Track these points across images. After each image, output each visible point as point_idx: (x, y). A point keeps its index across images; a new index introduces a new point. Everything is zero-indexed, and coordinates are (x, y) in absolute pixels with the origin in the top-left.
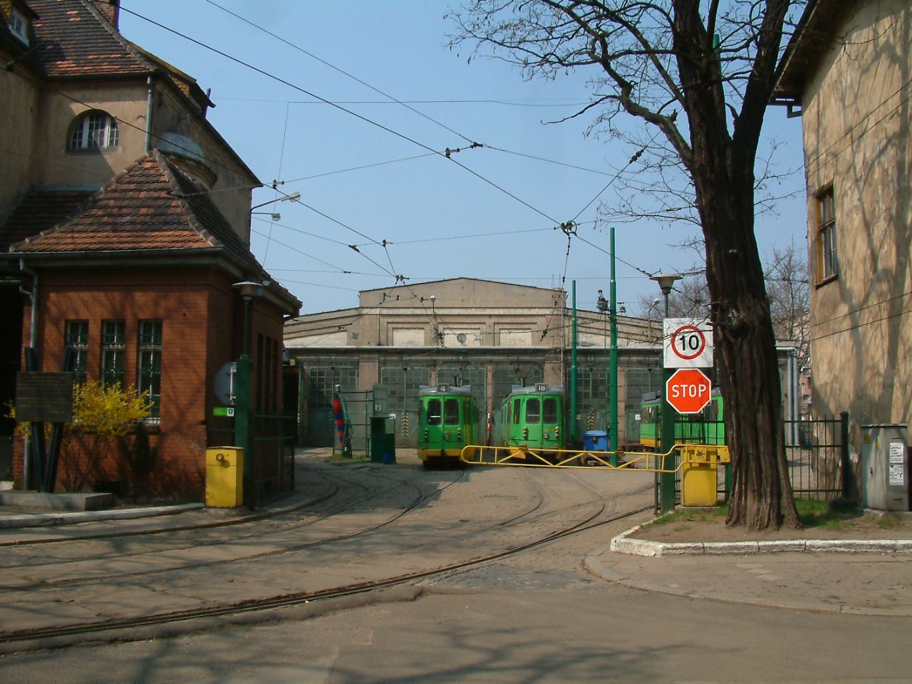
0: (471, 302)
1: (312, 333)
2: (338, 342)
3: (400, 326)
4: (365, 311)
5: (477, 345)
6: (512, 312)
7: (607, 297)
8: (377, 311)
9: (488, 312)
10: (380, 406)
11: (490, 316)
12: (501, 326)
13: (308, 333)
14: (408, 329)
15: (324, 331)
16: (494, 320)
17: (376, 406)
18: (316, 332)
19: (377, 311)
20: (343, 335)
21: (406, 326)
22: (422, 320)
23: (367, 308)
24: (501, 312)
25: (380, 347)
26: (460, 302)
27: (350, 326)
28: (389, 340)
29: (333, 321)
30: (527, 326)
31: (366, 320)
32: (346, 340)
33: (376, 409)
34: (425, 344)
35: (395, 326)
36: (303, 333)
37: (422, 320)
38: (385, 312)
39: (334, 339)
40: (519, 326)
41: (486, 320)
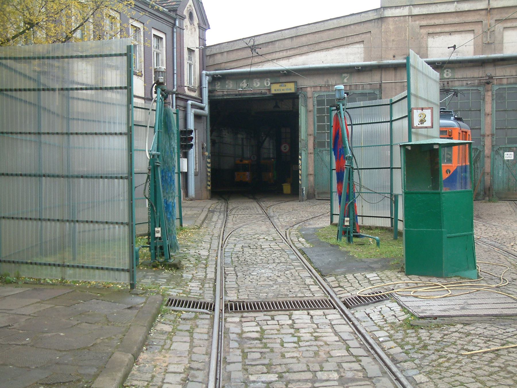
1: (317, 47)
2: (352, 58)
3: (438, 30)
4: (388, 13)
8: (405, 11)
13: (312, 48)
14: (450, 33)
15: (333, 43)
18: (323, 45)
19: (405, 11)
21: (447, 29)
22: (470, 18)
23: (391, 7)
27: (368, 35)
29: (344, 30)
31: (391, 25)
32: (363, 55)
34: (475, 53)
35: (431, 30)
36: (305, 49)
37: (470, 18)
38: (416, 11)
39: (347, 54)
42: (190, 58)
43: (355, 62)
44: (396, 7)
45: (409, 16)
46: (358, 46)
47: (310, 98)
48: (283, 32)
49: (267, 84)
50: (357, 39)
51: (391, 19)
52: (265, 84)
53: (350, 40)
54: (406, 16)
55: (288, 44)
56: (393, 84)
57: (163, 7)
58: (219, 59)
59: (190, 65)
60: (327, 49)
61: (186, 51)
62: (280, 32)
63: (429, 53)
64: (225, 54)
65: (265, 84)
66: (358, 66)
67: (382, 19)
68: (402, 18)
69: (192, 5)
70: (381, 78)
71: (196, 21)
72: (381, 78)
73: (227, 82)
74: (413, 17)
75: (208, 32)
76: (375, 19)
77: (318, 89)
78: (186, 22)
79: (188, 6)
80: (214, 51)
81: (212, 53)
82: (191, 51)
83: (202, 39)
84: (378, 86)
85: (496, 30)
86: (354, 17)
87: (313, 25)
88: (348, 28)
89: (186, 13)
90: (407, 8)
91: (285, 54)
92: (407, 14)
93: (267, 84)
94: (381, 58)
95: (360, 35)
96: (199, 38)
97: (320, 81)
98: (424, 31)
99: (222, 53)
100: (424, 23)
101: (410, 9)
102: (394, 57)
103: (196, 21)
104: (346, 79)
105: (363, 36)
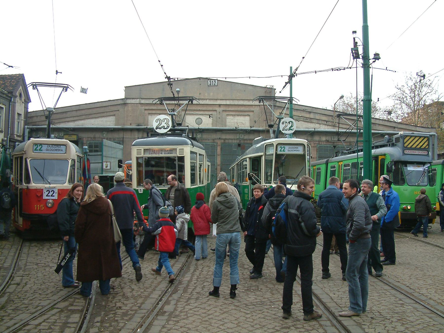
0: (206, 94)
1: (90, 117)
2: (109, 123)
3: (154, 112)
4: (129, 101)
5: (210, 127)
6: (236, 103)
7: (360, 43)
8: (137, 101)
9: (219, 102)
10: (109, 163)
11: (220, 105)
12: (228, 113)
16: (222, 108)
17: (104, 164)
18: (93, 116)
19: (137, 101)
20: (112, 119)
23: (130, 98)
24: (228, 102)
25: (139, 127)
26: (198, 94)
27: (118, 112)
28: (146, 122)
29: (105, 108)
30: (246, 113)
31: (130, 108)
33: (104, 167)
35: (150, 112)
36: (84, 117)
38: (143, 101)
39: (106, 121)
40: (241, 113)
41: (217, 109)
42: (18, 119)
43: (110, 126)
44: (133, 99)
45: (139, 104)
46: (112, 117)
47: (85, 144)
48: (72, 107)
49: (62, 135)
50: (112, 114)
51: (130, 104)
52: (61, 135)
53: (108, 114)
54: (138, 103)
55: (74, 114)
56: (130, 139)
57: (5, 90)
58: (35, 119)
59: (18, 122)
60: (96, 118)
61: (16, 115)
62: (70, 107)
63: (149, 123)
64: (39, 117)
65: (61, 135)
66: (111, 128)
67: (125, 104)
68: (135, 104)
69: (22, 89)
70: (124, 135)
71: (23, 98)
72: (124, 135)
73: (39, 132)
74: (141, 105)
75: (30, 104)
76: (121, 104)
77: (90, 139)
78: (18, 99)
79: (19, 90)
80: (33, 115)
81: (31, 116)
82: (19, 115)
83: (26, 108)
84: (122, 139)
85: (182, 114)
86: (111, 102)
87: (89, 104)
88: (107, 107)
89: (18, 94)
90: (139, 99)
91: (72, 119)
92: (138, 103)
93: (62, 135)
94: (124, 125)
95: (113, 112)
96: (25, 107)
97: (91, 135)
98: (147, 112)
99: (37, 116)
100: (147, 108)
101: (140, 100)
102: (131, 124)
103: (23, 98)
104: (105, 134)
105: (115, 112)
